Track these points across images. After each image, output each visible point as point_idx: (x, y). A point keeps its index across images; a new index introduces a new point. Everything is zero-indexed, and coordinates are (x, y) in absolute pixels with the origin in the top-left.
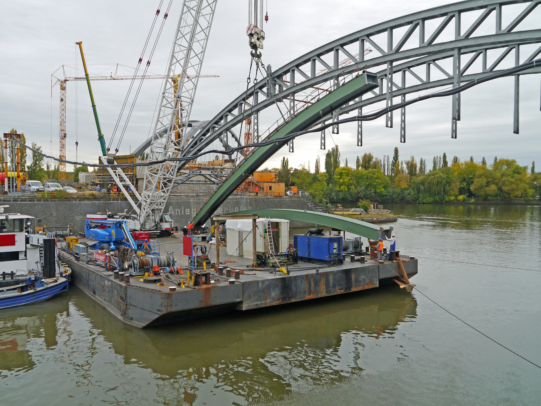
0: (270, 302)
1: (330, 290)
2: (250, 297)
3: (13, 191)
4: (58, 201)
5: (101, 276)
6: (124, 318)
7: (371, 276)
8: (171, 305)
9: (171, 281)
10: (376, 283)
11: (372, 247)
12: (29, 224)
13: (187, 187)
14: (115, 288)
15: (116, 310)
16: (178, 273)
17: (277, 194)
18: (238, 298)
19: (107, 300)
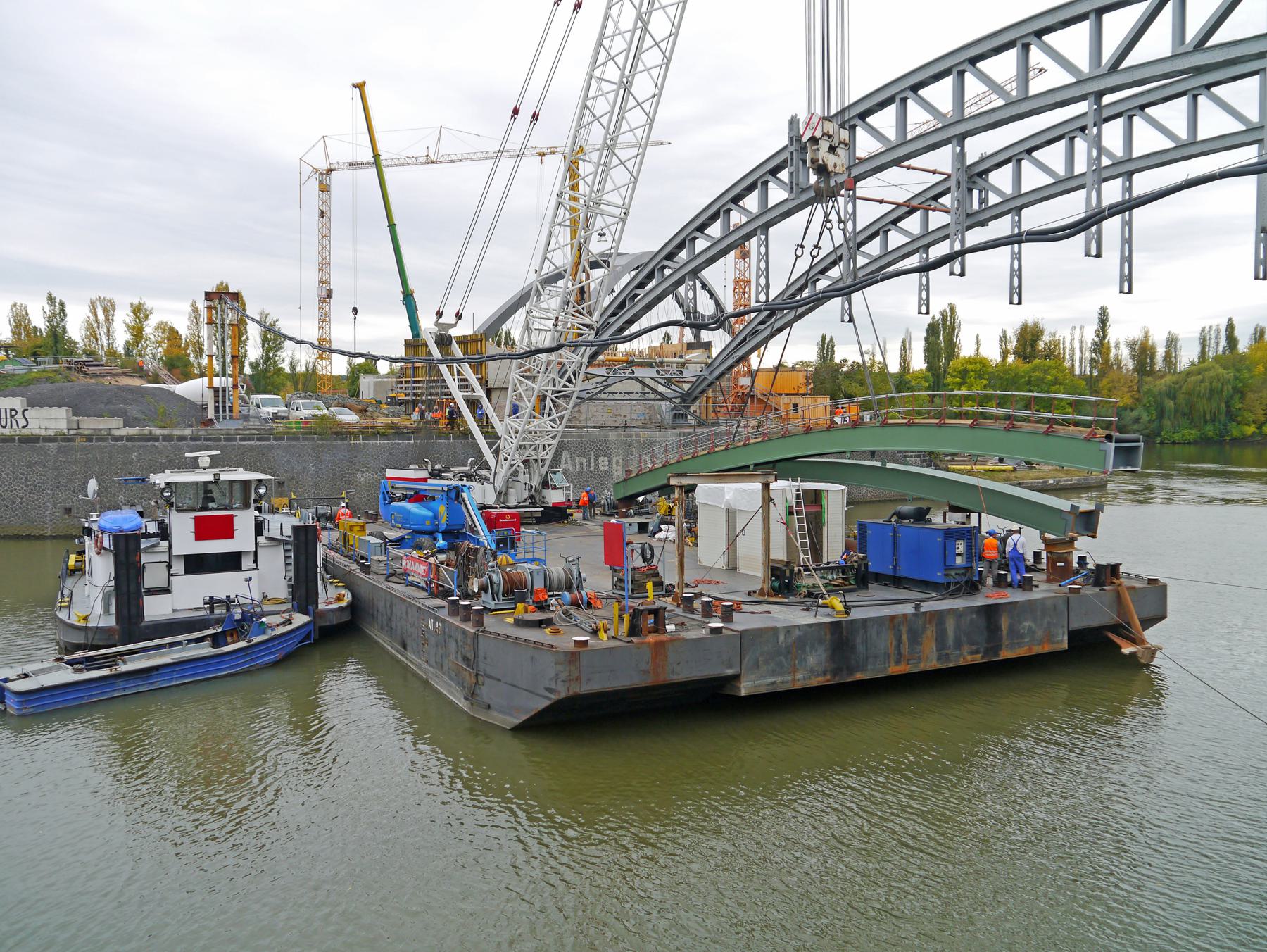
0: (804, 679)
1: (947, 654)
2: (757, 666)
3: (224, 418)
4: (318, 439)
5: (419, 608)
6: (472, 704)
7: (1049, 623)
8: (577, 680)
9: (576, 625)
10: (1062, 641)
11: (1051, 553)
12: (262, 491)
13: (600, 407)
14: (450, 637)
15: (453, 684)
16: (589, 605)
18: (730, 667)
19: (434, 664)
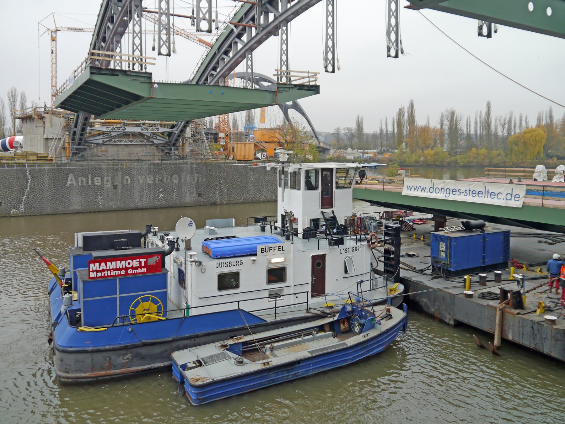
17: (242, 157)
